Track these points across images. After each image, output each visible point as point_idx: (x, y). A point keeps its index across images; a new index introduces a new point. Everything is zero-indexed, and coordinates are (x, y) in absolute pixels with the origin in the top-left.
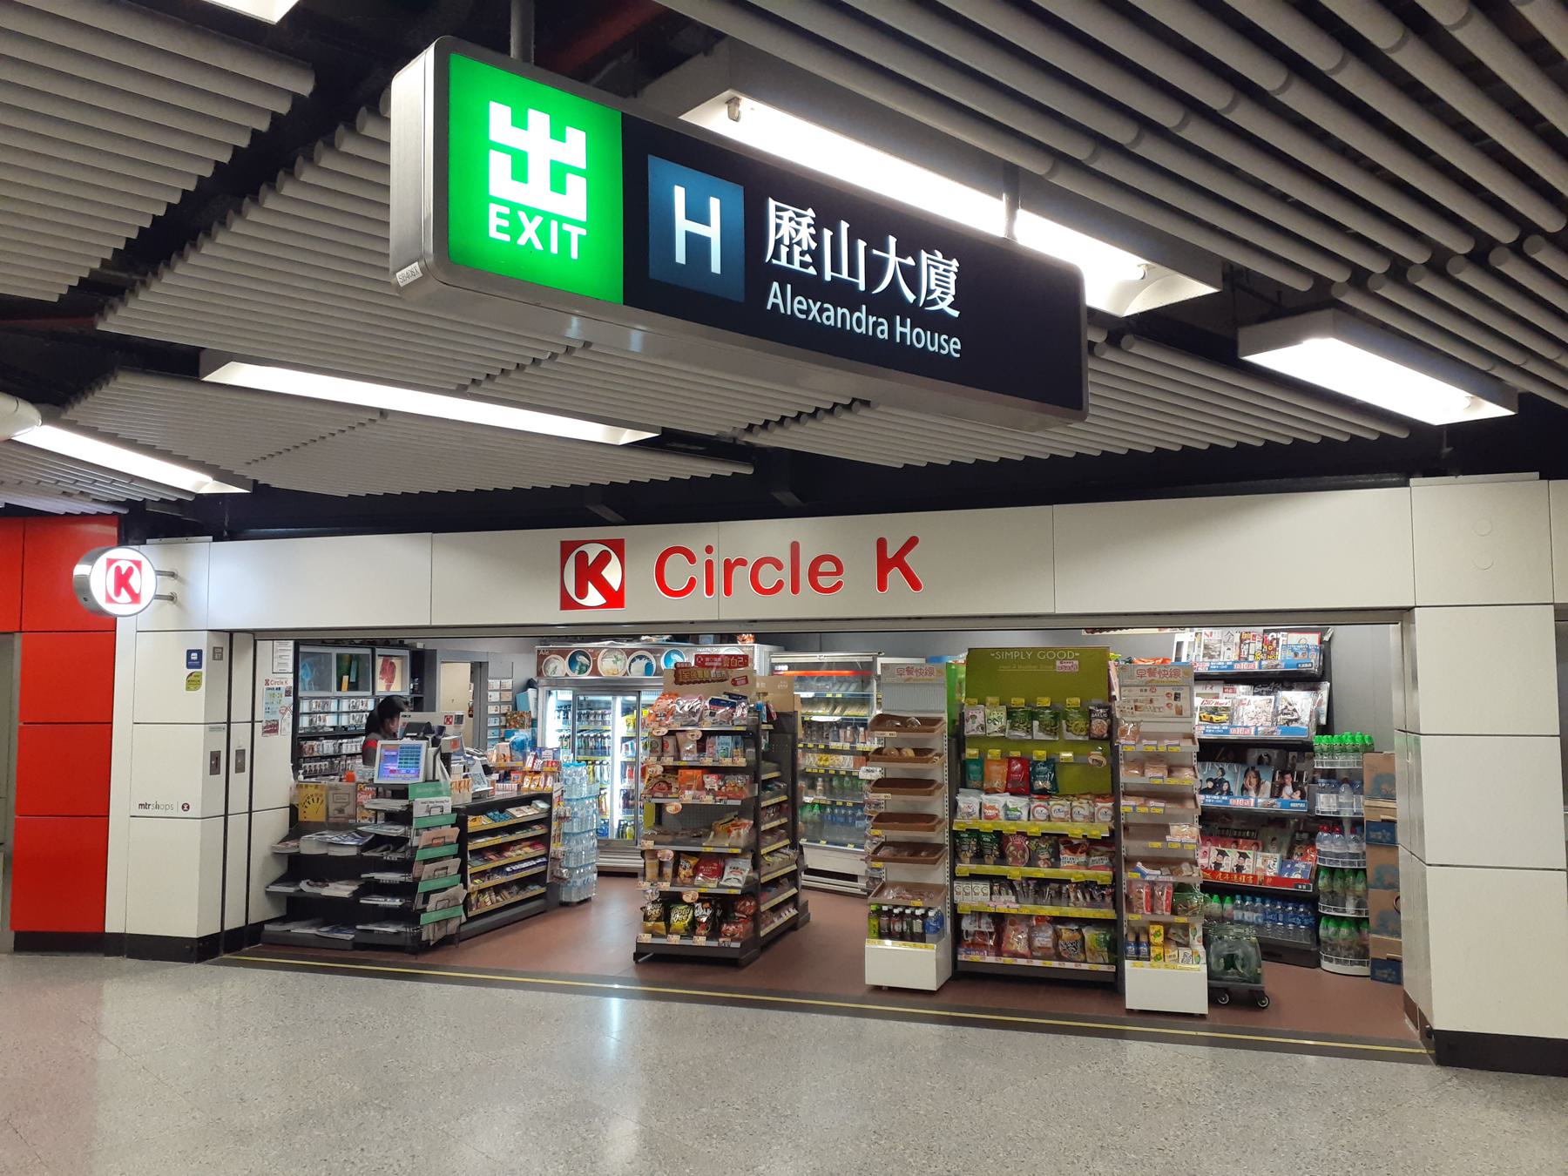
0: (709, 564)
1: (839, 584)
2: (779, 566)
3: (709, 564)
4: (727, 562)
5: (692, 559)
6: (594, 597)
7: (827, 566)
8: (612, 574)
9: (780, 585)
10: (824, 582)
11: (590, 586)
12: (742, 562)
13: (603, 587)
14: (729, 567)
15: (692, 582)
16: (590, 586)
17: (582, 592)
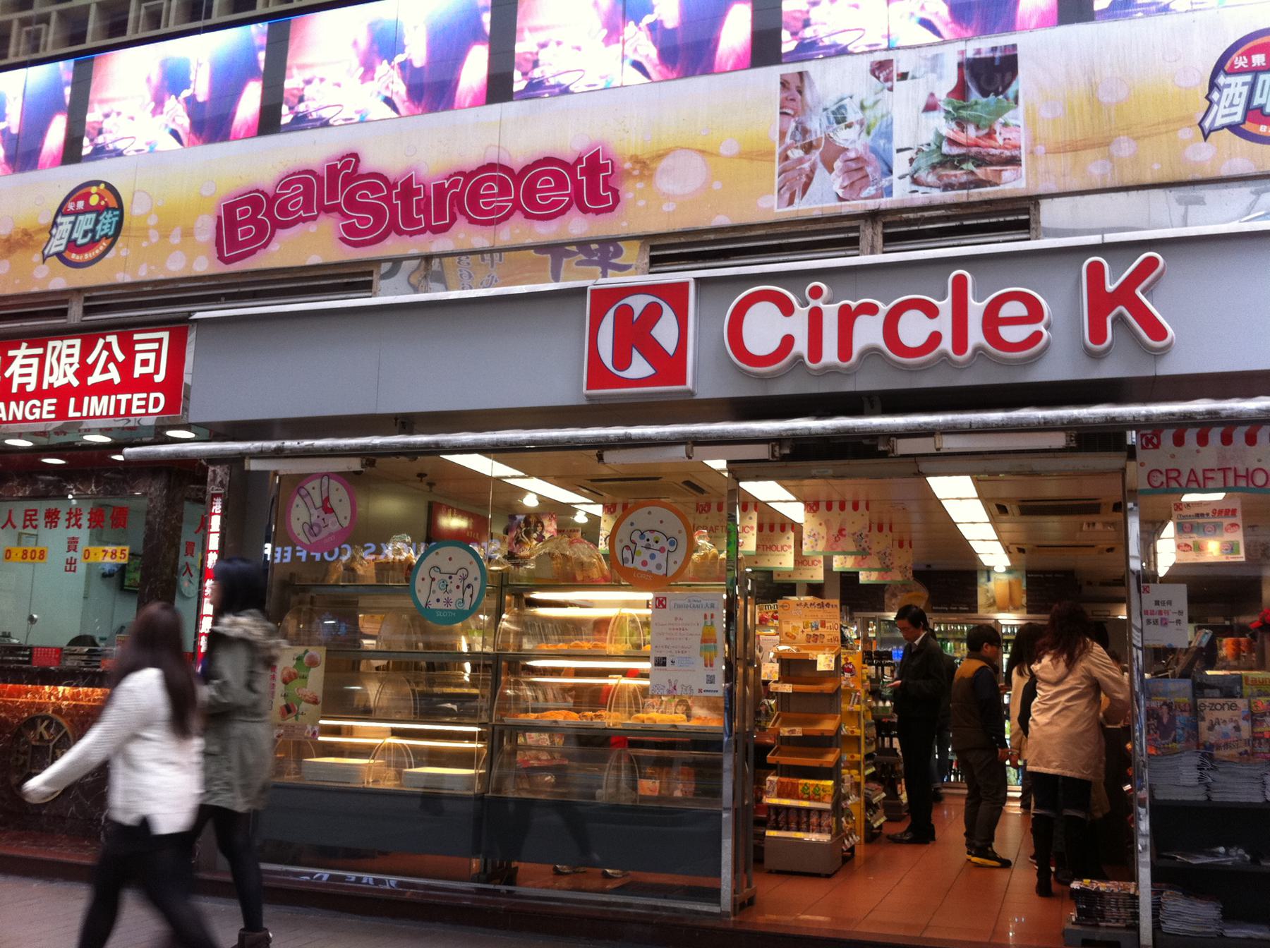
0: (816, 317)
1: (1037, 336)
2: (932, 311)
3: (816, 317)
4: (845, 311)
5: (787, 309)
6: (640, 367)
7: (1014, 309)
8: (665, 332)
9: (935, 338)
10: (1012, 334)
11: (635, 353)
12: (871, 310)
13: (653, 351)
14: (847, 319)
15: (788, 341)
16: (635, 353)
17: (622, 360)
